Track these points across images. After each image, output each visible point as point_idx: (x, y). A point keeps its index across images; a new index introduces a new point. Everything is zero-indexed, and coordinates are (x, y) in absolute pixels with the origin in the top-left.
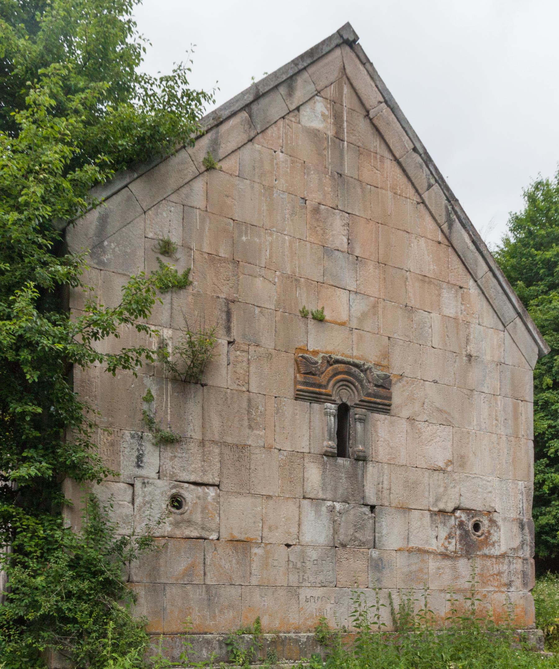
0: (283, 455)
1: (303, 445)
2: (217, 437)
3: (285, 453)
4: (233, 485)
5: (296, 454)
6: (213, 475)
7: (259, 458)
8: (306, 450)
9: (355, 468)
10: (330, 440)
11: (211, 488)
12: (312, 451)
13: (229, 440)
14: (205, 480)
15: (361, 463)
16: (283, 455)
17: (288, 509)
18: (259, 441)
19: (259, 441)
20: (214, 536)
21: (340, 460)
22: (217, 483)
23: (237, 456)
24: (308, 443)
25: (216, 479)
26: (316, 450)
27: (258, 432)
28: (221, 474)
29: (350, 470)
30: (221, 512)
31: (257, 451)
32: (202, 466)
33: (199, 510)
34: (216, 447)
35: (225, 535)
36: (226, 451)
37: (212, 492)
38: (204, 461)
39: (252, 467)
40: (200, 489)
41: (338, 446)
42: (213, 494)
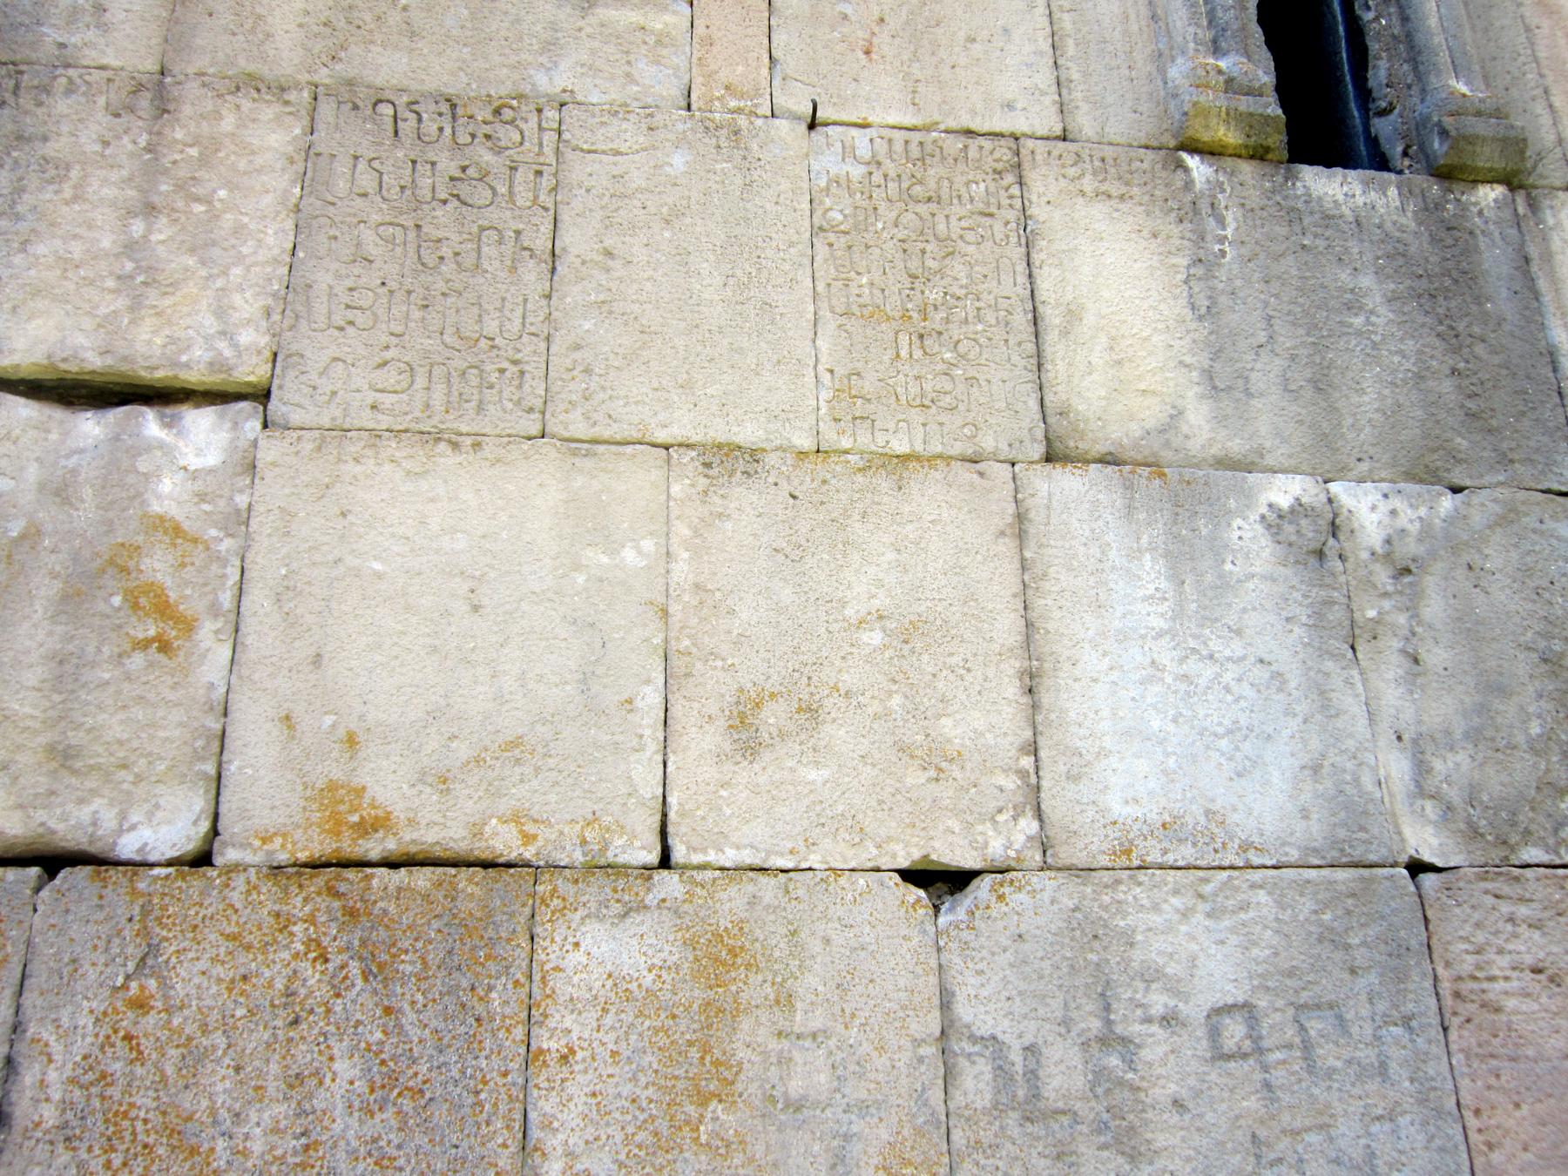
0: (848, 152)
1: (1008, 86)
2: (286, 53)
3: (861, 139)
4: (389, 377)
5: (954, 145)
6: (221, 312)
7: (637, 180)
8: (1039, 118)
9: (1452, 234)
10: (1216, 49)
11: (200, 422)
12: (1085, 123)
13: (389, 66)
14: (147, 351)
15: (1489, 195)
16: (848, 152)
17: (933, 544)
18: (645, 70)
19: (645, 70)
20: (166, 830)
21: (1330, 187)
22: (251, 372)
23: (448, 165)
24: (1045, 78)
25: (246, 337)
26: (1115, 112)
27: (633, 17)
28: (291, 294)
29: (1419, 246)
30: (258, 600)
31: (630, 134)
32: (130, 248)
33: (45, 590)
34: (268, 112)
35: (270, 807)
36: (346, 137)
37: (203, 436)
38: (150, 210)
39: (575, 240)
40: (91, 426)
41: (1284, 90)
42: (212, 459)
